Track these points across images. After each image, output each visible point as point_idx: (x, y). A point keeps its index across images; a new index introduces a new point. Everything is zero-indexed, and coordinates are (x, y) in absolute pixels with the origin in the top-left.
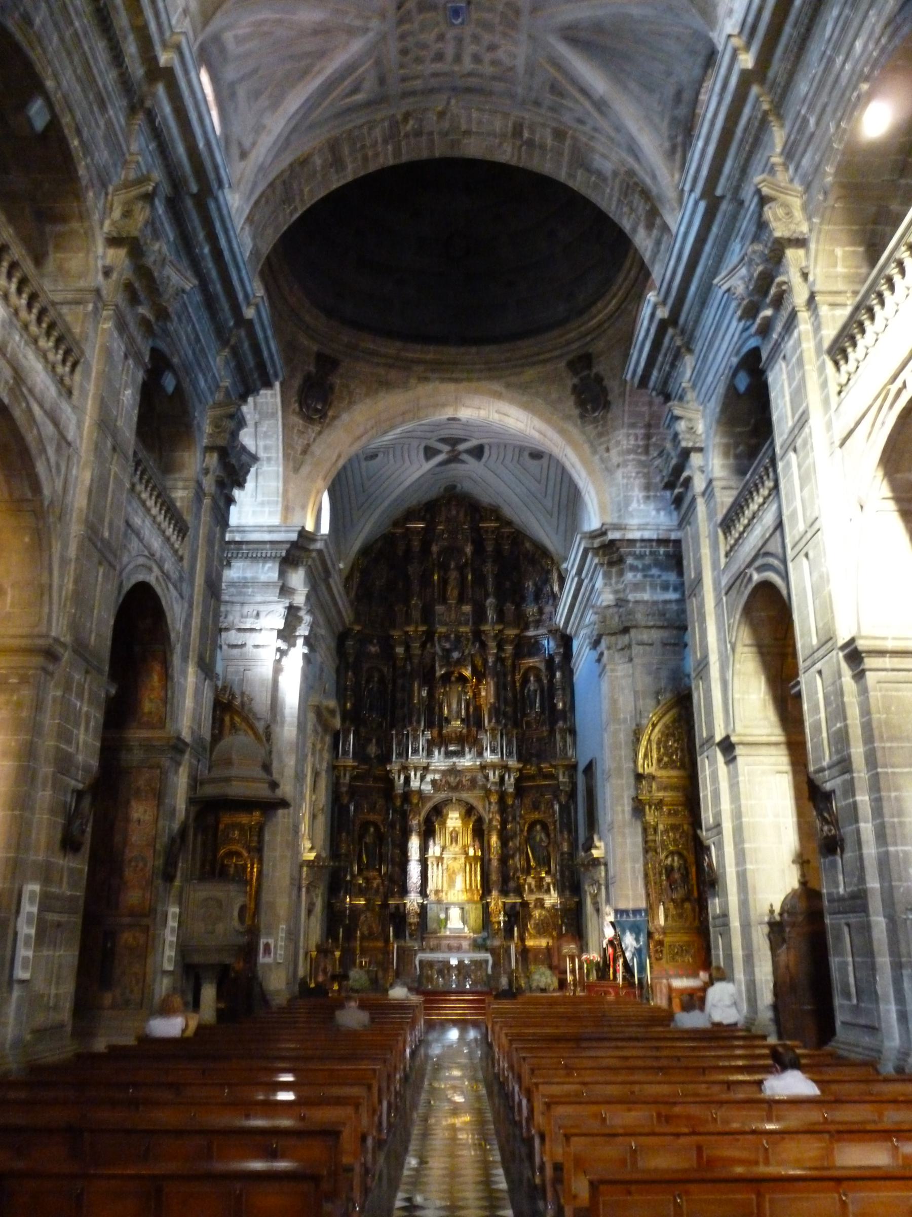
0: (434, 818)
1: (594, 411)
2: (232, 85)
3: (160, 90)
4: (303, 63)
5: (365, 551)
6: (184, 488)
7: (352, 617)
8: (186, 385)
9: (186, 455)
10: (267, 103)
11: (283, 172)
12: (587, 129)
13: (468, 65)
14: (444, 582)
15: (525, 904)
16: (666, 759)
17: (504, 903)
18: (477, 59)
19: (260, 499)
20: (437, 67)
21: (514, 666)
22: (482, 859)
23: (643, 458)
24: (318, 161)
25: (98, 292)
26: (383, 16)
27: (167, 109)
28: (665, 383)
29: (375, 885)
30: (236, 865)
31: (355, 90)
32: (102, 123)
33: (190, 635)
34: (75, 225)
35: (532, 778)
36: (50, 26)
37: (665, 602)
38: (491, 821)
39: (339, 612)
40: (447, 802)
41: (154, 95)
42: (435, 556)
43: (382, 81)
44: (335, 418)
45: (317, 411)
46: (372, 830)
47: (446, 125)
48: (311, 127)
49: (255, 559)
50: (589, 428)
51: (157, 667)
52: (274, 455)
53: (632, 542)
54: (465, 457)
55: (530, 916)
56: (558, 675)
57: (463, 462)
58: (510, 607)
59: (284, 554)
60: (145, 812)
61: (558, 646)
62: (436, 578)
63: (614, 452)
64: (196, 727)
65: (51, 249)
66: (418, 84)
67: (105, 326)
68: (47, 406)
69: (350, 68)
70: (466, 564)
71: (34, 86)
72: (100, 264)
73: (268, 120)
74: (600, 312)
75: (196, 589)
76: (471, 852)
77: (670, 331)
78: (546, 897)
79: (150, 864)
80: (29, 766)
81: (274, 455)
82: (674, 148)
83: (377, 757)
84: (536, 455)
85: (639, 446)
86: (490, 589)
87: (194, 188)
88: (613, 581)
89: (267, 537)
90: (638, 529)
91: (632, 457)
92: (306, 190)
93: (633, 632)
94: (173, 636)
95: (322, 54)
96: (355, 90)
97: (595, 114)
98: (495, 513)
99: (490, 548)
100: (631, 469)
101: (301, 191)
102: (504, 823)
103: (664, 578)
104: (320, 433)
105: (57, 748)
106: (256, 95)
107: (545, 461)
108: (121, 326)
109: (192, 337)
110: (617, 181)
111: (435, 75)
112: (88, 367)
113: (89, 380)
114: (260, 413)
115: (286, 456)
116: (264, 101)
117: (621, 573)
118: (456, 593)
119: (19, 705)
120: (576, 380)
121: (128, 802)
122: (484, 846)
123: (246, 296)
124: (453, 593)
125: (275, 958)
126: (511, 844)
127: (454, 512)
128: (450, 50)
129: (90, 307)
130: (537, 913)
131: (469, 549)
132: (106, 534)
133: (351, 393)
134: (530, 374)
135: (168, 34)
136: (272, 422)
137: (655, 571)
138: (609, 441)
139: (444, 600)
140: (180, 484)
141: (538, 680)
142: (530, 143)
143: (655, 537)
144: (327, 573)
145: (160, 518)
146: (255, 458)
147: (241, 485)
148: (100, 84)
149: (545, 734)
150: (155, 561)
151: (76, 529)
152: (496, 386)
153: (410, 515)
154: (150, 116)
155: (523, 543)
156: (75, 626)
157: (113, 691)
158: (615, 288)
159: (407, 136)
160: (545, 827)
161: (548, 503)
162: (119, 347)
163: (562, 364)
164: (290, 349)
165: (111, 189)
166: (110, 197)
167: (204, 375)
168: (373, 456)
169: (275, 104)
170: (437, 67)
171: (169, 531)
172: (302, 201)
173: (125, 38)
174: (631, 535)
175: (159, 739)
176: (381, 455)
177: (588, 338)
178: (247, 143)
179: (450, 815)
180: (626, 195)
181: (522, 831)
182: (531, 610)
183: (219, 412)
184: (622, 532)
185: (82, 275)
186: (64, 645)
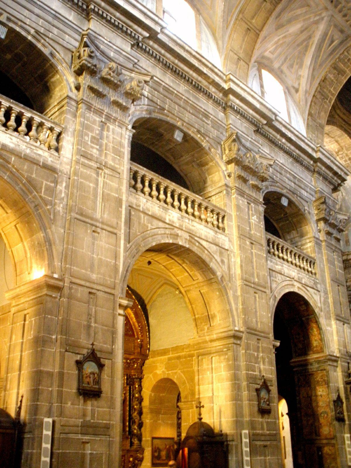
2: (279, 68)
3: (231, 97)
4: (305, 44)
6: (310, 242)
8: (294, 199)
9: (307, 227)
10: (297, 67)
11: (317, 89)
24: (331, 76)
25: (226, 185)
26: (326, 9)
27: (238, 101)
31: (332, 42)
32: (209, 122)
33: (329, 307)
34: (211, 164)
36: (173, 105)
41: (230, 100)
43: (342, 31)
48: (321, 65)
51: (314, 325)
60: (323, 390)
64: (342, 348)
65: (207, 175)
67: (234, 196)
68: (210, 240)
69: (325, 35)
71: (172, 128)
72: (226, 173)
73: (301, 73)
75: (328, 285)
79: (330, 415)
80: (235, 383)
87: (265, 122)
92: (332, 89)
94: (317, 310)
95: (310, 37)
101: (330, 91)
105: (247, 374)
106: (292, 66)
108: (241, 193)
109: (292, 178)
112: (230, 215)
113: (232, 221)
116: (296, 67)
119: (228, 360)
121: (315, 388)
123: (313, 149)
129: (225, 192)
132: (256, 280)
135: (224, 77)
140: (308, 241)
148: (203, 110)
150: (295, 280)
151: (239, 283)
156: (245, 322)
157: (278, 344)
162: (243, 202)
165: (222, 143)
166: (223, 146)
167: (305, 190)
169: (301, 66)
172: (333, 95)
173: (209, 88)
175: (322, 357)
178: (296, 85)
183: (318, 203)
185: (220, 180)
186: (242, 332)
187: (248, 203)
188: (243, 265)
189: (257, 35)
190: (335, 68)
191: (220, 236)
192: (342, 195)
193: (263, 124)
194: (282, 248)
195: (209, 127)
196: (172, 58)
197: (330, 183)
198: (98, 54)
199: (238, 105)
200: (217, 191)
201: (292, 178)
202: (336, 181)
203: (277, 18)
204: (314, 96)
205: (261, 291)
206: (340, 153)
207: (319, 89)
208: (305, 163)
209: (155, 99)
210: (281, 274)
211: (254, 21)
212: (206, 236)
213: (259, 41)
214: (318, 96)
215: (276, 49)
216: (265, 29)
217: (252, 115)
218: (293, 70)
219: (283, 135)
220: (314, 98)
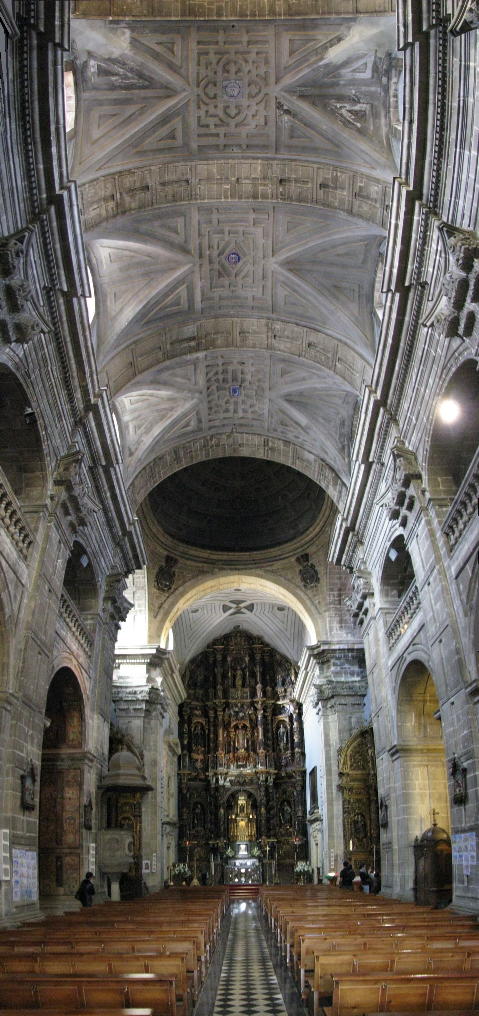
0: (231, 800)
1: (311, 583)
2: (127, 422)
3: (91, 415)
5: (192, 661)
6: (92, 619)
7: (186, 696)
8: (94, 563)
11: (150, 463)
12: (301, 440)
13: (240, 414)
14: (234, 677)
18: (245, 411)
20: (226, 415)
21: (272, 719)
23: (338, 606)
24: (168, 458)
26: (201, 393)
27: (93, 424)
28: (350, 561)
32: (59, 426)
36: (39, 379)
39: (179, 692)
43: (200, 421)
44: (176, 589)
45: (166, 586)
47: (231, 441)
50: (309, 592)
53: (334, 651)
54: (244, 610)
57: (243, 613)
61: (295, 709)
66: (217, 423)
69: (185, 415)
70: (245, 668)
74: (311, 533)
76: (251, 817)
77: (351, 534)
81: (143, 609)
82: (343, 448)
84: (281, 609)
85: (335, 600)
86: (259, 679)
87: (104, 463)
88: (325, 671)
90: (337, 644)
91: (332, 606)
95: (172, 409)
96: (187, 425)
97: (304, 433)
98: (260, 639)
99: (258, 657)
100: (332, 613)
101: (159, 472)
103: (352, 669)
104: (168, 597)
106: (139, 427)
107: (285, 612)
109: (99, 540)
110: (317, 464)
111: (224, 418)
115: (150, 609)
117: (329, 668)
118: (240, 682)
120: (301, 568)
124: (239, 682)
127: (239, 640)
128: (232, 408)
131: (247, 659)
133: (184, 577)
134: (277, 565)
137: (347, 666)
139: (234, 686)
140: (90, 617)
141: (285, 727)
142: (272, 449)
143: (346, 647)
144: (173, 672)
145: (77, 634)
146: (132, 605)
147: (123, 619)
152: (259, 571)
153: (215, 642)
154: (84, 426)
158: (318, 521)
159: (212, 446)
163: (293, 559)
164: (153, 554)
168: (196, 611)
170: (226, 415)
171: (82, 641)
172: (160, 477)
173: (76, 391)
174: (334, 647)
176: (200, 610)
177: (306, 546)
178: (133, 449)
180: (322, 470)
182: (280, 690)
187: (60, 542)
188: (37, 612)
189: (135, 375)
190: (176, 452)
191: (21, 563)
193: (101, 465)
194: (71, 612)
195: (56, 432)
196: (67, 333)
197: (127, 564)
198: (22, 261)
199: (91, 428)
200: (31, 509)
201: (99, 540)
202: (132, 565)
203: (158, 371)
204: (144, 468)
205: (45, 653)
207: (152, 464)
208: (115, 530)
209: (29, 360)
210: (63, 641)
211: (140, 359)
212: (8, 555)
213: (133, 382)
214: (147, 471)
215: (137, 402)
216: (145, 373)
217: (97, 448)
218: (139, 432)
219: (112, 488)
220: (144, 471)
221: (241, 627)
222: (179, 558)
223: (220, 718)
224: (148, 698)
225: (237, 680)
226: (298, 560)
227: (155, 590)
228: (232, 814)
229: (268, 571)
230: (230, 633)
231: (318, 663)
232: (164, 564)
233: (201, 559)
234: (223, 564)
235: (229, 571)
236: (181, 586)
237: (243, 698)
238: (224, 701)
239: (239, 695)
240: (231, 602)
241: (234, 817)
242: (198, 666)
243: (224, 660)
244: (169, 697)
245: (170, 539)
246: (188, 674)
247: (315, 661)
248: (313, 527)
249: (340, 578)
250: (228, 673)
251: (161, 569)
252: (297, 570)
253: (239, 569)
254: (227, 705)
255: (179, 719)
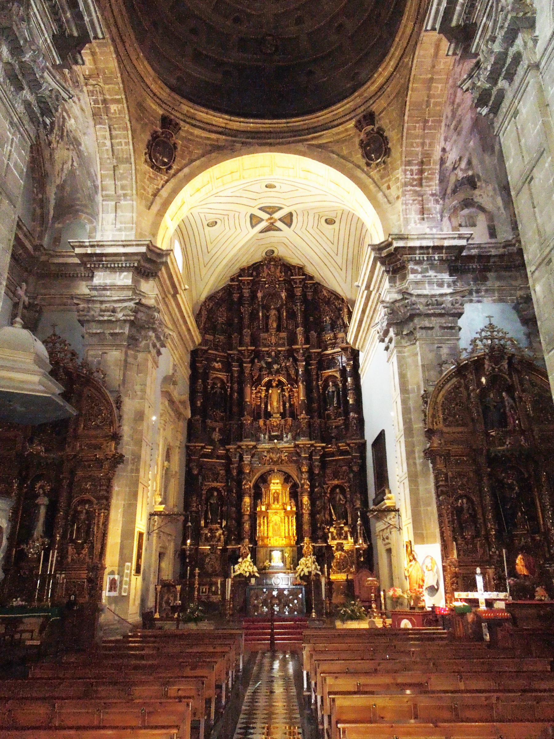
0: (261, 485)
5: (211, 298)
7: (200, 341)
14: (266, 317)
15: (329, 547)
16: (451, 419)
17: (313, 546)
19: (118, 226)
21: (317, 374)
22: (297, 514)
23: (418, 189)
29: (217, 534)
30: (87, 512)
35: (332, 454)
37: (442, 295)
38: (303, 485)
39: (189, 330)
40: (270, 472)
42: (260, 299)
45: (164, 164)
46: (215, 494)
49: (113, 270)
50: (373, 173)
52: (129, 192)
53: (412, 249)
54: (279, 224)
55: (333, 557)
56: (349, 379)
57: (279, 230)
58: (313, 334)
59: (136, 265)
61: (349, 360)
62: (261, 314)
63: (393, 188)
70: (282, 306)
76: (289, 508)
78: (344, 542)
83: (220, 441)
85: (414, 179)
86: (299, 320)
88: (398, 284)
89: (122, 250)
90: (418, 239)
91: (409, 188)
93: (416, 320)
98: (301, 269)
99: (298, 292)
100: (409, 198)
102: (312, 487)
104: (167, 182)
114: (116, 159)
115: (141, 196)
117: (404, 278)
118: (275, 325)
122: (299, 505)
125: (120, 593)
126: (318, 502)
127: (273, 269)
130: (337, 554)
131: (283, 295)
136: (128, 165)
137: (431, 273)
138: (390, 180)
139: (266, 329)
141: (335, 385)
143: (431, 244)
144: (176, 292)
149: (341, 422)
152: (301, 147)
155: (322, 291)
160: (343, 491)
161: (339, 260)
163: (352, 124)
174: (411, 244)
176: (219, 222)
179: (273, 481)
181: (325, 493)
182: (328, 336)
184: (404, 242)
192: (72, 165)
206: (91, 81)
221: (275, 254)
222: (182, 123)
223: (247, 371)
224: (132, 318)
225: (270, 321)
226: (359, 126)
227: (147, 168)
228: (262, 504)
229: (313, 145)
230: (261, 262)
231: (388, 272)
232: (159, 129)
233: (214, 128)
234: (248, 138)
235: (257, 147)
236: (186, 166)
237: (277, 345)
238: (253, 348)
239: (273, 341)
240: (261, 209)
241: (263, 508)
242: (218, 305)
243: (253, 296)
244: (170, 326)
245: (168, 90)
246: (204, 313)
247: (383, 268)
248: (384, 65)
249: (423, 144)
250: (258, 313)
251: (155, 136)
252: (357, 141)
253: (270, 144)
254: (258, 355)
255: (190, 372)
